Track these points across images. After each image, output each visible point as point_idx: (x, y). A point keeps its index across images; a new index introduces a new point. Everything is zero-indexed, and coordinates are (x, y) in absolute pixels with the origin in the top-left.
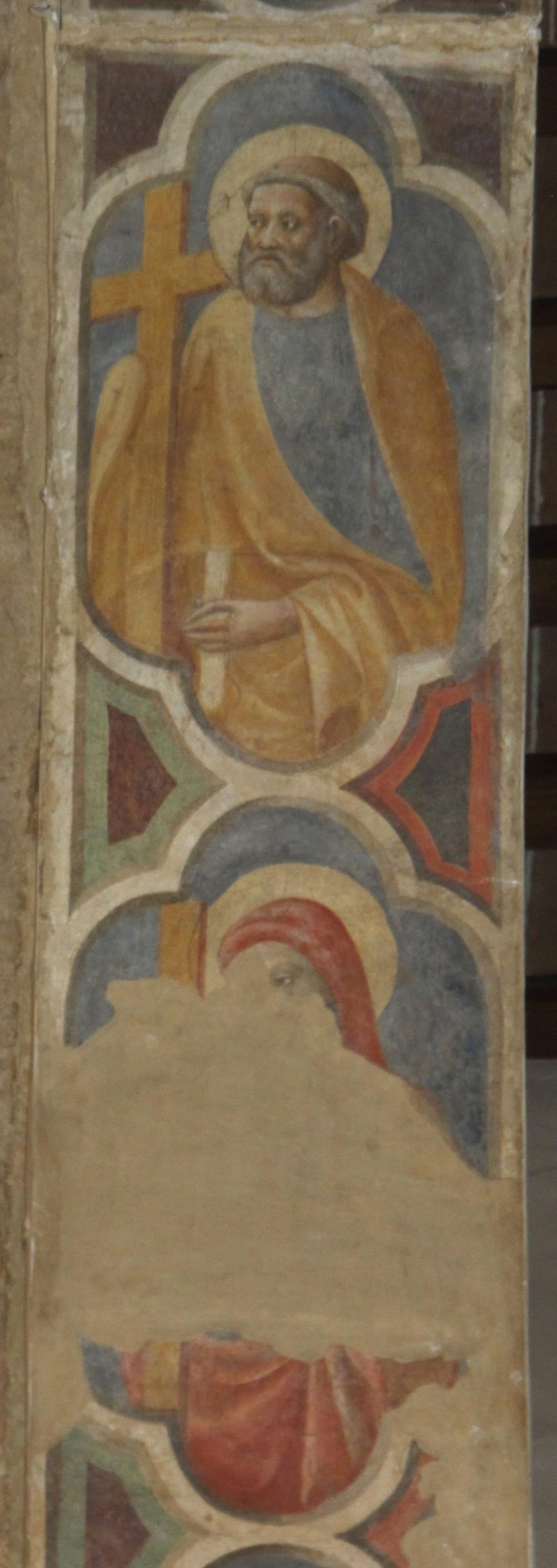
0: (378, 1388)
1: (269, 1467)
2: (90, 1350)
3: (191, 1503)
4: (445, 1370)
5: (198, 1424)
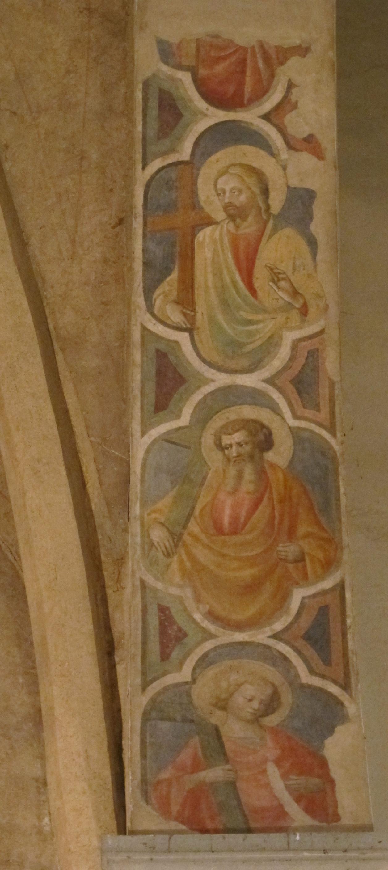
0: (275, 57)
1: (231, 89)
2: (160, 42)
3: (201, 104)
4: (303, 50)
5: (203, 72)
